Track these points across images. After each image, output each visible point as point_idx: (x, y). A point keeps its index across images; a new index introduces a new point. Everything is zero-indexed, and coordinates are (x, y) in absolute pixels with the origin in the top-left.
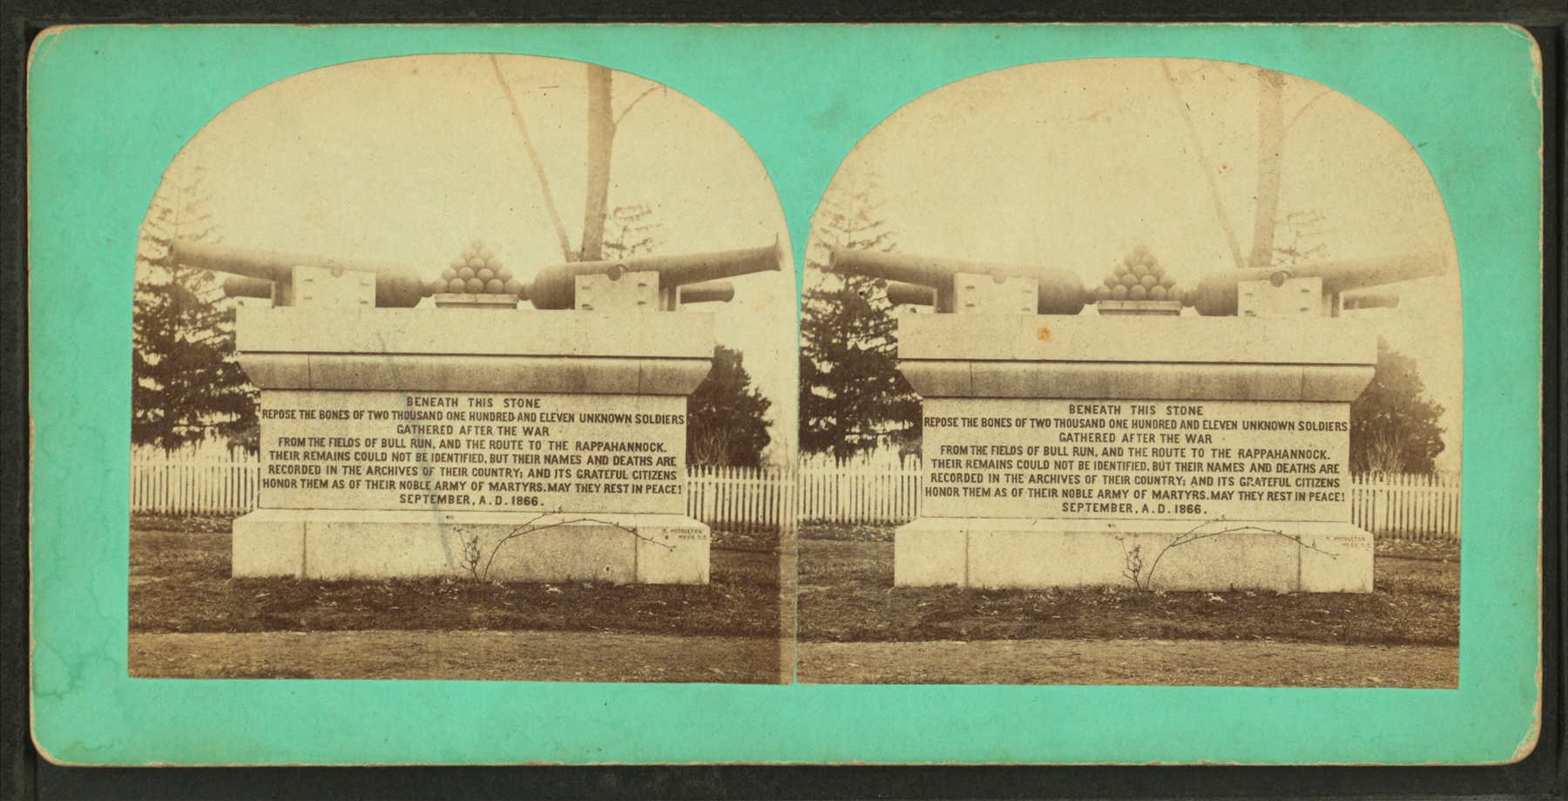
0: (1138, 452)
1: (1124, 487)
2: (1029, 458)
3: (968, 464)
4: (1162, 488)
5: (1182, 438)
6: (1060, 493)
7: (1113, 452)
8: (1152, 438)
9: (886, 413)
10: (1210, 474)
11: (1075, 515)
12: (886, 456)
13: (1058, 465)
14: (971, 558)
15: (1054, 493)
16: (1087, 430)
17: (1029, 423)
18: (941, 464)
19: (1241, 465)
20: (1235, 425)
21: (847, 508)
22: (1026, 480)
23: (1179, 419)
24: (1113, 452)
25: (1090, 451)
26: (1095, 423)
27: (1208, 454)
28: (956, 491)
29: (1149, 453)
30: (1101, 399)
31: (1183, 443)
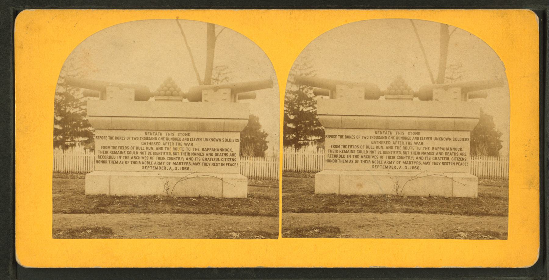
0: (168, 149)
1: (163, 161)
2: (131, 150)
3: (110, 152)
4: (176, 161)
5: (183, 144)
6: (141, 163)
7: (160, 149)
8: (173, 144)
9: (79, 134)
10: (192, 156)
11: (146, 170)
12: (79, 149)
13: (141, 153)
14: (111, 185)
15: (139, 163)
16: (151, 141)
17: (131, 138)
18: (101, 152)
19: (203, 153)
20: (201, 140)
21: (67, 167)
22: (130, 158)
23: (182, 137)
24: (160, 149)
25: (152, 148)
26: (154, 139)
27: (192, 149)
28: (106, 162)
29: (172, 149)
30: (156, 130)
31: (183, 146)
